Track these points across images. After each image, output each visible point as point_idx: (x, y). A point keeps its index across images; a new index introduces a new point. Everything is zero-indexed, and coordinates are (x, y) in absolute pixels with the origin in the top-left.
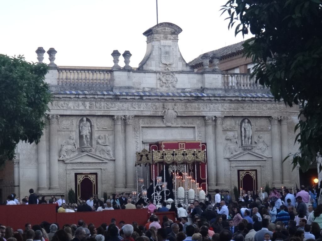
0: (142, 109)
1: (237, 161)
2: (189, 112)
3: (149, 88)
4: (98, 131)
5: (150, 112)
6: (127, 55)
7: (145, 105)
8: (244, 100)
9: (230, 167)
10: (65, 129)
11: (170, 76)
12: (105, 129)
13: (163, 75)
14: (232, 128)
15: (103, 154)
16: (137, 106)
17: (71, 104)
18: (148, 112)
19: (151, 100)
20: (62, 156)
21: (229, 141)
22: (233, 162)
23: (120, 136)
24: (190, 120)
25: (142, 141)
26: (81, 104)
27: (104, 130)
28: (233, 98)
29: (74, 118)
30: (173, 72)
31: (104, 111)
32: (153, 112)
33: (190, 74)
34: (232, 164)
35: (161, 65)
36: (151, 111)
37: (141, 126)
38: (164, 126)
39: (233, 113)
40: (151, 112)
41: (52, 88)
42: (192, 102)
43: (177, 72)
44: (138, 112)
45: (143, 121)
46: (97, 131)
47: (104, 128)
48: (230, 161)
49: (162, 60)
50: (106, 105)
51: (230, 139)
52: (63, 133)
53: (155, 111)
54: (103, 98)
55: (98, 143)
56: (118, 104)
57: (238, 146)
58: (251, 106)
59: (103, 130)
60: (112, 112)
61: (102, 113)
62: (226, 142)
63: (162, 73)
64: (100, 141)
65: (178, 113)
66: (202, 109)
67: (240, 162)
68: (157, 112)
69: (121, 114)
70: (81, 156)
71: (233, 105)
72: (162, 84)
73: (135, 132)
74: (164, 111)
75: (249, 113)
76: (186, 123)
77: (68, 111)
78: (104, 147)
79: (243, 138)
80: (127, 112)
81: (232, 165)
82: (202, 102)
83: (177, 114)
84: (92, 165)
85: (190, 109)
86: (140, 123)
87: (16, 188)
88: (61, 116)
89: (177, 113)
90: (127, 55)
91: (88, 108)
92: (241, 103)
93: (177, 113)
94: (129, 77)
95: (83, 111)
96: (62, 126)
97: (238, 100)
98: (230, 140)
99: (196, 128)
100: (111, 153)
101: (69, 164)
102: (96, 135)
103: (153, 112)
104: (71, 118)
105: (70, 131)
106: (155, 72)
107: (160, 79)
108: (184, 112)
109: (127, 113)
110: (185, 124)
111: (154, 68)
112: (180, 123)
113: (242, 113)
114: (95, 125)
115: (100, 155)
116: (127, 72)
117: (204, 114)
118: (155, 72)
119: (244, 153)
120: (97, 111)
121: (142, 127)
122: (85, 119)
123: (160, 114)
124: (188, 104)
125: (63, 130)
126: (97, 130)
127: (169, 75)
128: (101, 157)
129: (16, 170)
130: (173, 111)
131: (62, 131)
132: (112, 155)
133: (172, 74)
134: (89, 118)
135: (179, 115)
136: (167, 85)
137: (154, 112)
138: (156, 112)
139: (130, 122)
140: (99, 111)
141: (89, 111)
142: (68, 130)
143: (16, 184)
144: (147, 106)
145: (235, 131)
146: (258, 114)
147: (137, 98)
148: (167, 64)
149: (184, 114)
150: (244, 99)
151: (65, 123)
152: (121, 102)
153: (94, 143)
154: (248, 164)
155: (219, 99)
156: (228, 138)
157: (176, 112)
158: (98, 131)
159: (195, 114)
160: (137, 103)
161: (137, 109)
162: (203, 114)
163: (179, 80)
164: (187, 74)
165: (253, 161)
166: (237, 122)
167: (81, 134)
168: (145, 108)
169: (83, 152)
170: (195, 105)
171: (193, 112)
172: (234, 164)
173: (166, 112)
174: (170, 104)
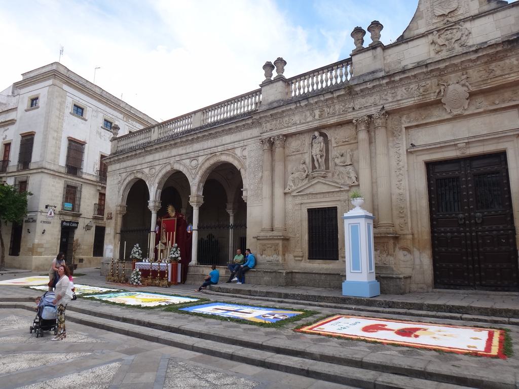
0: (399, 98)
3: (415, 63)
4: (339, 146)
5: (413, 99)
6: (376, 26)
7: (405, 91)
10: (294, 152)
11: (455, 31)
12: (345, 141)
13: (438, 34)
15: (343, 178)
16: (390, 95)
17: (297, 118)
18: (410, 100)
19: (412, 78)
20: (288, 187)
23: (363, 146)
24: (508, 94)
25: (407, 151)
26: (309, 115)
27: (346, 143)
29: (306, 135)
30: (456, 23)
31: (339, 116)
32: (418, 98)
33: (498, 13)
36: (414, 97)
37: (403, 126)
40: (416, 99)
41: (274, 103)
42: (501, 59)
43: (465, 20)
44: (391, 104)
45: (407, 118)
46: (336, 147)
47: (344, 140)
49: (435, 11)
50: (341, 107)
52: (294, 157)
53: (423, 95)
54: (333, 98)
55: (336, 165)
56: (359, 102)
59: (343, 144)
60: (349, 114)
61: (336, 120)
63: (438, 31)
64: (337, 161)
65: (470, 87)
68: (427, 96)
69: (365, 112)
70: (311, 184)
72: (438, 49)
73: (395, 138)
74: (438, 91)
76: (497, 102)
77: (293, 128)
78: (342, 169)
80: (373, 109)
83: (469, 89)
84: (327, 196)
85: (498, 72)
86: (402, 121)
88: (287, 136)
89: (467, 87)
90: (376, 26)
91: (317, 117)
93: (467, 87)
94: (375, 57)
95: (310, 123)
96: (292, 149)
100: (353, 175)
101: (299, 197)
102: (334, 153)
103: (418, 98)
104: (302, 137)
105: (301, 153)
106: (423, 36)
107: (433, 43)
108: (485, 82)
109: (373, 111)
111: (422, 30)
112: (483, 104)
114: (333, 141)
115: (338, 181)
116: (371, 51)
118: (423, 36)
120: (328, 119)
121: (407, 128)
122: (317, 134)
123: (432, 97)
124: (493, 66)
125: (293, 154)
126: (335, 145)
127: (451, 29)
128: (337, 183)
131: (292, 155)
132: (354, 179)
133: (457, 26)
134: (324, 131)
135: (473, 89)
136: (449, 47)
137: (421, 97)
138: (424, 97)
139: (379, 122)
140: (331, 118)
141: (318, 122)
142: (298, 152)
144: (407, 91)
147: (384, 81)
148: (445, 13)
149: (485, 85)
151: (294, 144)
152: (363, 97)
153: (331, 164)
157: (463, 85)
158: (339, 146)
160: (389, 92)
163: (473, 31)
164: (491, 16)
168: (404, 94)
169: (314, 178)
171: (507, 76)
173: (442, 90)
174: (453, 75)
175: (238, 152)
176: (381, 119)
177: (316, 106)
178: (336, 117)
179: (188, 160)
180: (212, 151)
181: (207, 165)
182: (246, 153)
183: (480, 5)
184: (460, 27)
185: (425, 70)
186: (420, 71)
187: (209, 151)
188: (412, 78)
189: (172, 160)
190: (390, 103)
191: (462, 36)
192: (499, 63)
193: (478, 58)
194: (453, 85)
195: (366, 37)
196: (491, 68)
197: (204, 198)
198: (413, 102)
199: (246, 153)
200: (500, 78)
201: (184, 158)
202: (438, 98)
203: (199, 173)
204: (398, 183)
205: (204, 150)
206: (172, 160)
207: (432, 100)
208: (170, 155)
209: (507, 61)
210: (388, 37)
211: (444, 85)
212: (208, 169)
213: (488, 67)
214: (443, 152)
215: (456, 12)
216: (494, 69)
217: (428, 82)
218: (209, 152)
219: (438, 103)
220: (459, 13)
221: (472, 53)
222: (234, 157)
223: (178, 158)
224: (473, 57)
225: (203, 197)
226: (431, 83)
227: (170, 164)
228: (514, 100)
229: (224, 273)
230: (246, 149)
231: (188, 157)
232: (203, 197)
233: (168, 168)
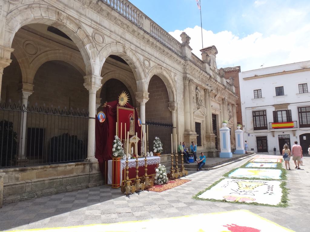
35: (214, 68)
87: (175, 130)
129: (174, 115)
143: (175, 125)
167: (198, 97)
175: (173, 74)
180: (160, 64)
187: (158, 62)
189: (127, 45)
201: (140, 52)
203: (150, 74)
218: (158, 63)
222: (169, 76)
223: (133, 47)
227: (124, 47)
229: (167, 160)
231: (143, 54)
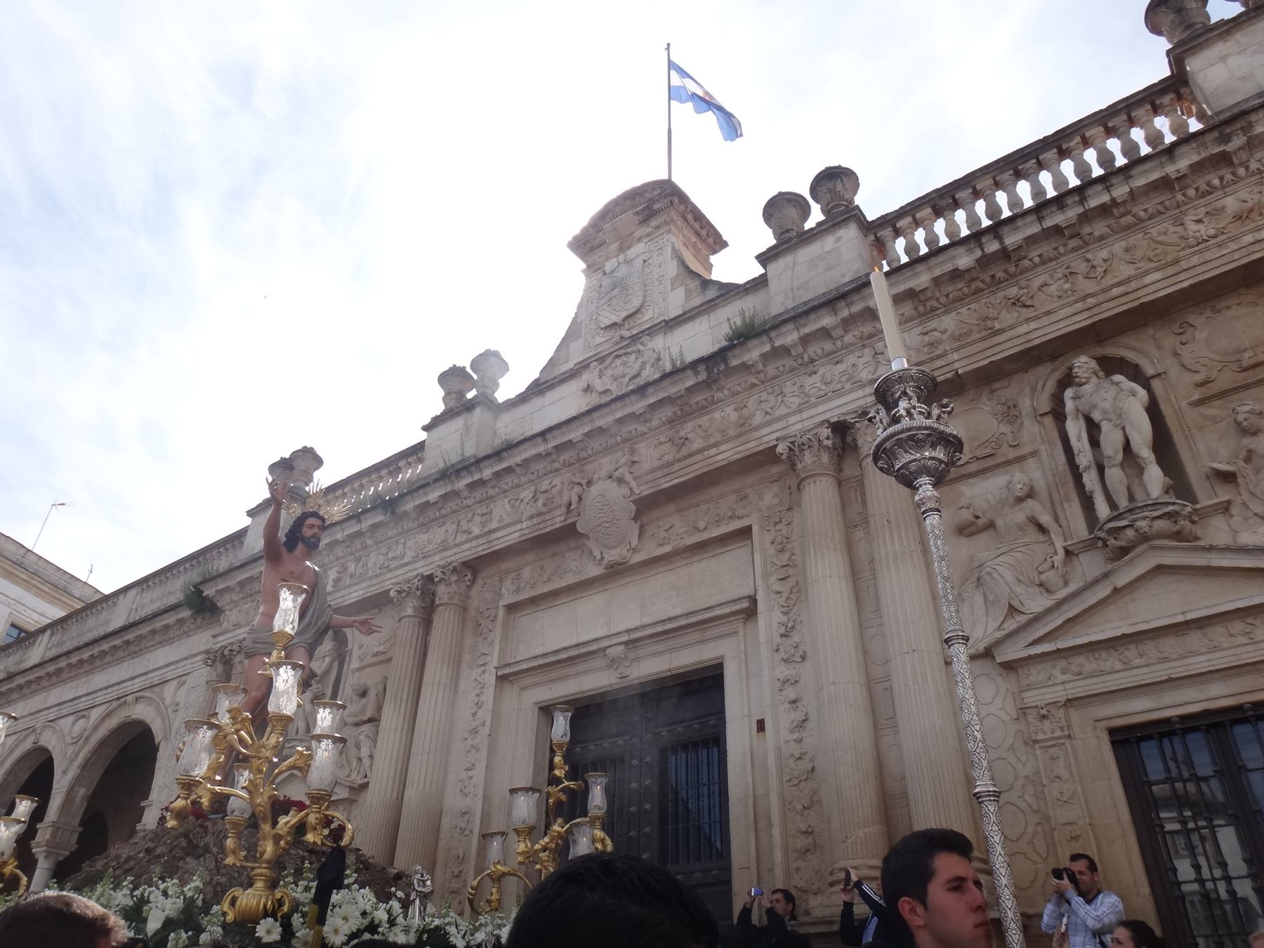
0: (494, 525)
1: (1078, 660)
2: (692, 460)
5: (519, 527)
8: (1005, 254)
9: (1023, 711)
14: (989, 451)
16: (478, 519)
19: (518, 470)
21: (983, 539)
22: (1036, 674)
28: (917, 275)
32: (529, 523)
34: (1030, 687)
37: (502, 603)
38: (594, 571)
39: (956, 356)
40: (524, 525)
42: (703, 409)
43: (652, 331)
48: (1009, 666)
51: (980, 522)
57: (1059, 544)
58: (1082, 267)
61: (361, 592)
62: (965, 547)
65: (633, 484)
66: (758, 419)
67: (1110, 661)
71: (948, 322)
75: (1080, 306)
76: (702, 525)
79: (1090, 480)
81: (1032, 698)
82: (754, 385)
85: (698, 444)
92: (996, 283)
97: (955, 275)
98: (991, 525)
99: (755, 528)
103: (529, 523)
108: (666, 471)
110: (696, 528)
112: (676, 528)
113: (1024, 329)
117: (767, 437)
119: (1121, 580)
121: (512, 608)
124: (688, 429)
130: (611, 486)
135: (646, 491)
137: (535, 521)
138: (541, 518)
144: (512, 507)
145: (1020, 459)
146: (1157, 285)
150: (992, 247)
154: (1193, 654)
155: (826, 320)
156: (966, 515)
157: (620, 481)
159: (727, 453)
161: (476, 531)
162: (766, 439)
165: (1237, 626)
166: (1025, 404)
170: (726, 414)
172: (1052, 686)
176: (449, 585)
177: (331, 557)
178: (363, 585)
179: (71, 718)
181: (103, 732)
182: (181, 696)
183: (686, 297)
184: (641, 348)
185: (541, 448)
186: (533, 452)
188: (518, 470)
190: (477, 537)
191: (642, 368)
192: (699, 421)
193: (653, 407)
194: (601, 482)
195: (463, 390)
196: (682, 434)
197: (81, 833)
198: (517, 535)
199: (181, 696)
200: (699, 457)
202: (569, 521)
204: (464, 775)
205: (106, 688)
206: (40, 721)
207: (557, 526)
208: (43, 706)
209: (717, 415)
210: (507, 389)
211: (580, 484)
212: (103, 743)
213: (678, 432)
214: (578, 674)
215: (639, 316)
216: (689, 436)
217: (557, 481)
219: (568, 535)
220: (645, 318)
221: (634, 398)
224: (639, 405)
225: (81, 829)
226: (559, 485)
228: (739, 518)
230: (184, 683)
232: (81, 829)
233: (28, 745)
